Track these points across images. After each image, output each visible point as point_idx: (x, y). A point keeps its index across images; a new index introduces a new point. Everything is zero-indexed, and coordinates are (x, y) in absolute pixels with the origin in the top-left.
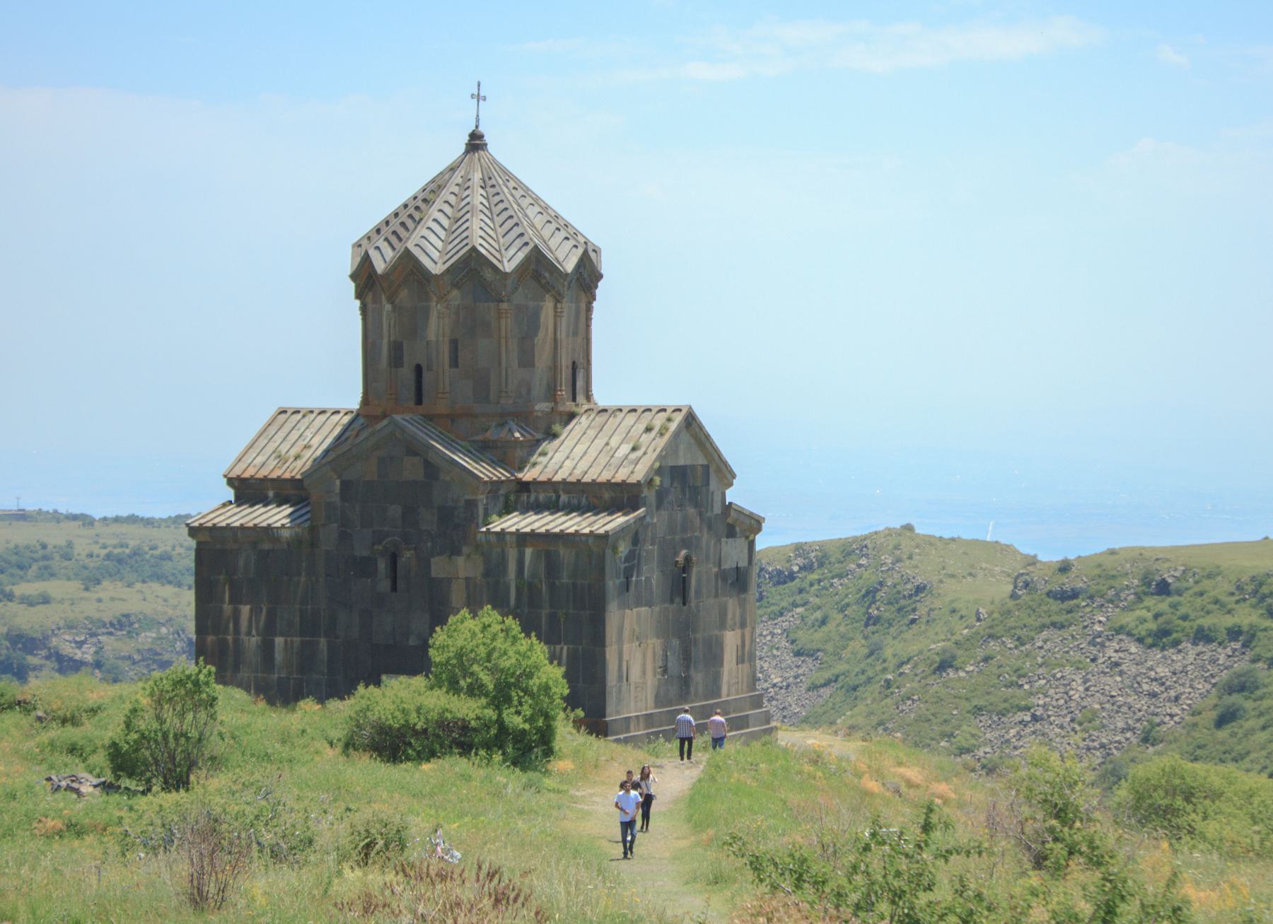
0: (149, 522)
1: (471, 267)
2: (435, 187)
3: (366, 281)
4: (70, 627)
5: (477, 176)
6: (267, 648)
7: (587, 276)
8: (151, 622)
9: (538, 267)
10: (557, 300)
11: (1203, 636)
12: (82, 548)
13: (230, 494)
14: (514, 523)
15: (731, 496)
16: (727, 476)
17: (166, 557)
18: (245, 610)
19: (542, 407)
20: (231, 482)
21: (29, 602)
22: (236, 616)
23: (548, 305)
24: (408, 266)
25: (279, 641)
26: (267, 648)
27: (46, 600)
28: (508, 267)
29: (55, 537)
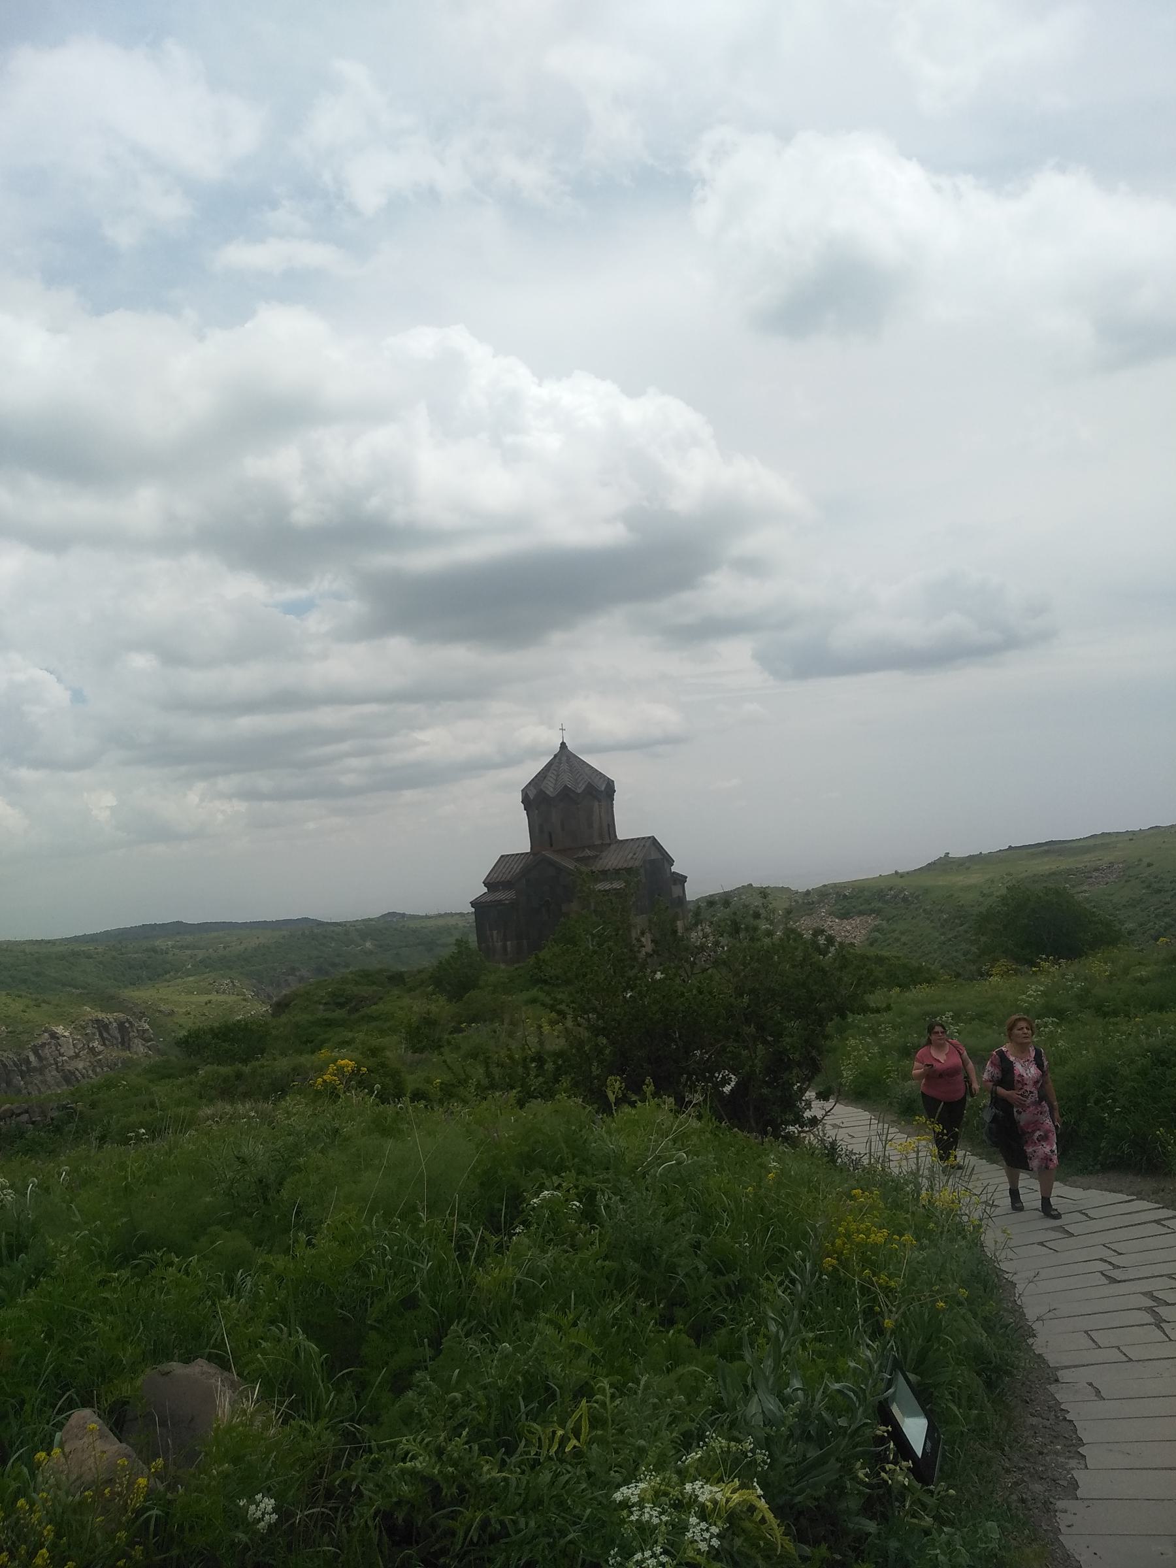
5: (564, 758)
6: (505, 948)
7: (609, 789)
10: (599, 801)
13: (486, 890)
15: (673, 869)
16: (671, 862)
18: (495, 932)
19: (598, 842)
20: (486, 884)
22: (492, 936)
23: (596, 804)
24: (541, 795)
25: (509, 943)
26: (505, 948)
28: (579, 791)
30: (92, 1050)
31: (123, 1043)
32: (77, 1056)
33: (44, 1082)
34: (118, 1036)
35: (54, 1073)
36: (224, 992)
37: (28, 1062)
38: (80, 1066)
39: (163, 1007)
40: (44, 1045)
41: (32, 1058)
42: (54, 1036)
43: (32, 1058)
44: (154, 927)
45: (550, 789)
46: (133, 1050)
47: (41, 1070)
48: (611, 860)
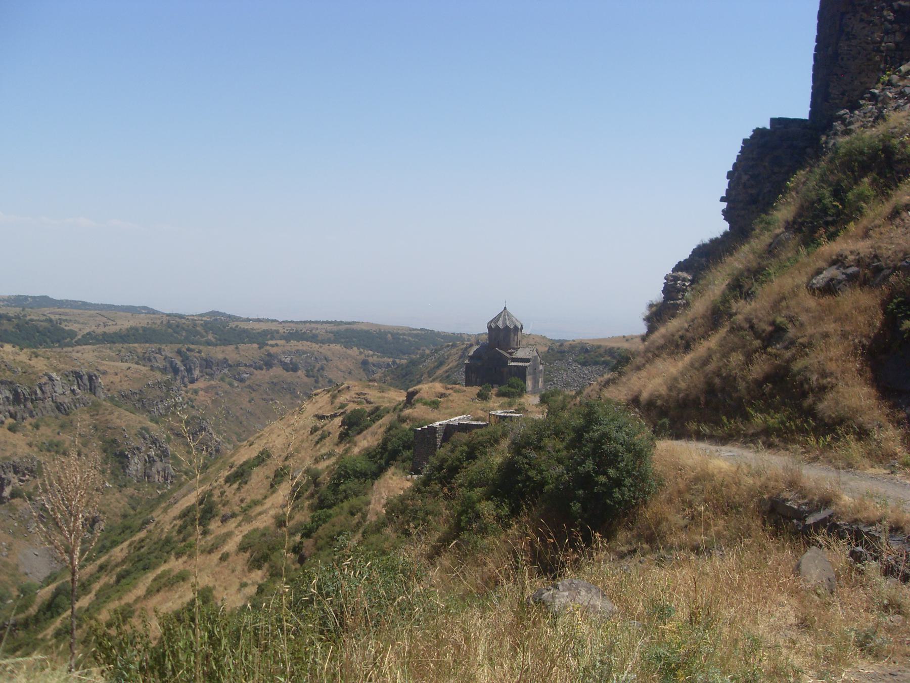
0: (296, 323)
1: (507, 328)
2: (500, 315)
3: (490, 328)
4: (284, 353)
7: (522, 327)
8: (305, 352)
9: (516, 328)
11: (596, 363)
12: (281, 331)
14: (512, 364)
17: (304, 333)
21: (272, 346)
24: (497, 327)
27: (277, 345)
29: (273, 327)
30: (73, 391)
31: (91, 389)
32: (64, 394)
33: (44, 408)
34: (88, 384)
35: (51, 403)
36: (126, 361)
37: (36, 394)
38: (66, 400)
39: (101, 368)
40: (45, 384)
41: (39, 392)
42: (51, 379)
43: (39, 392)
44: (222, 329)
45: (500, 324)
46: (97, 394)
47: (43, 400)
48: (520, 354)
